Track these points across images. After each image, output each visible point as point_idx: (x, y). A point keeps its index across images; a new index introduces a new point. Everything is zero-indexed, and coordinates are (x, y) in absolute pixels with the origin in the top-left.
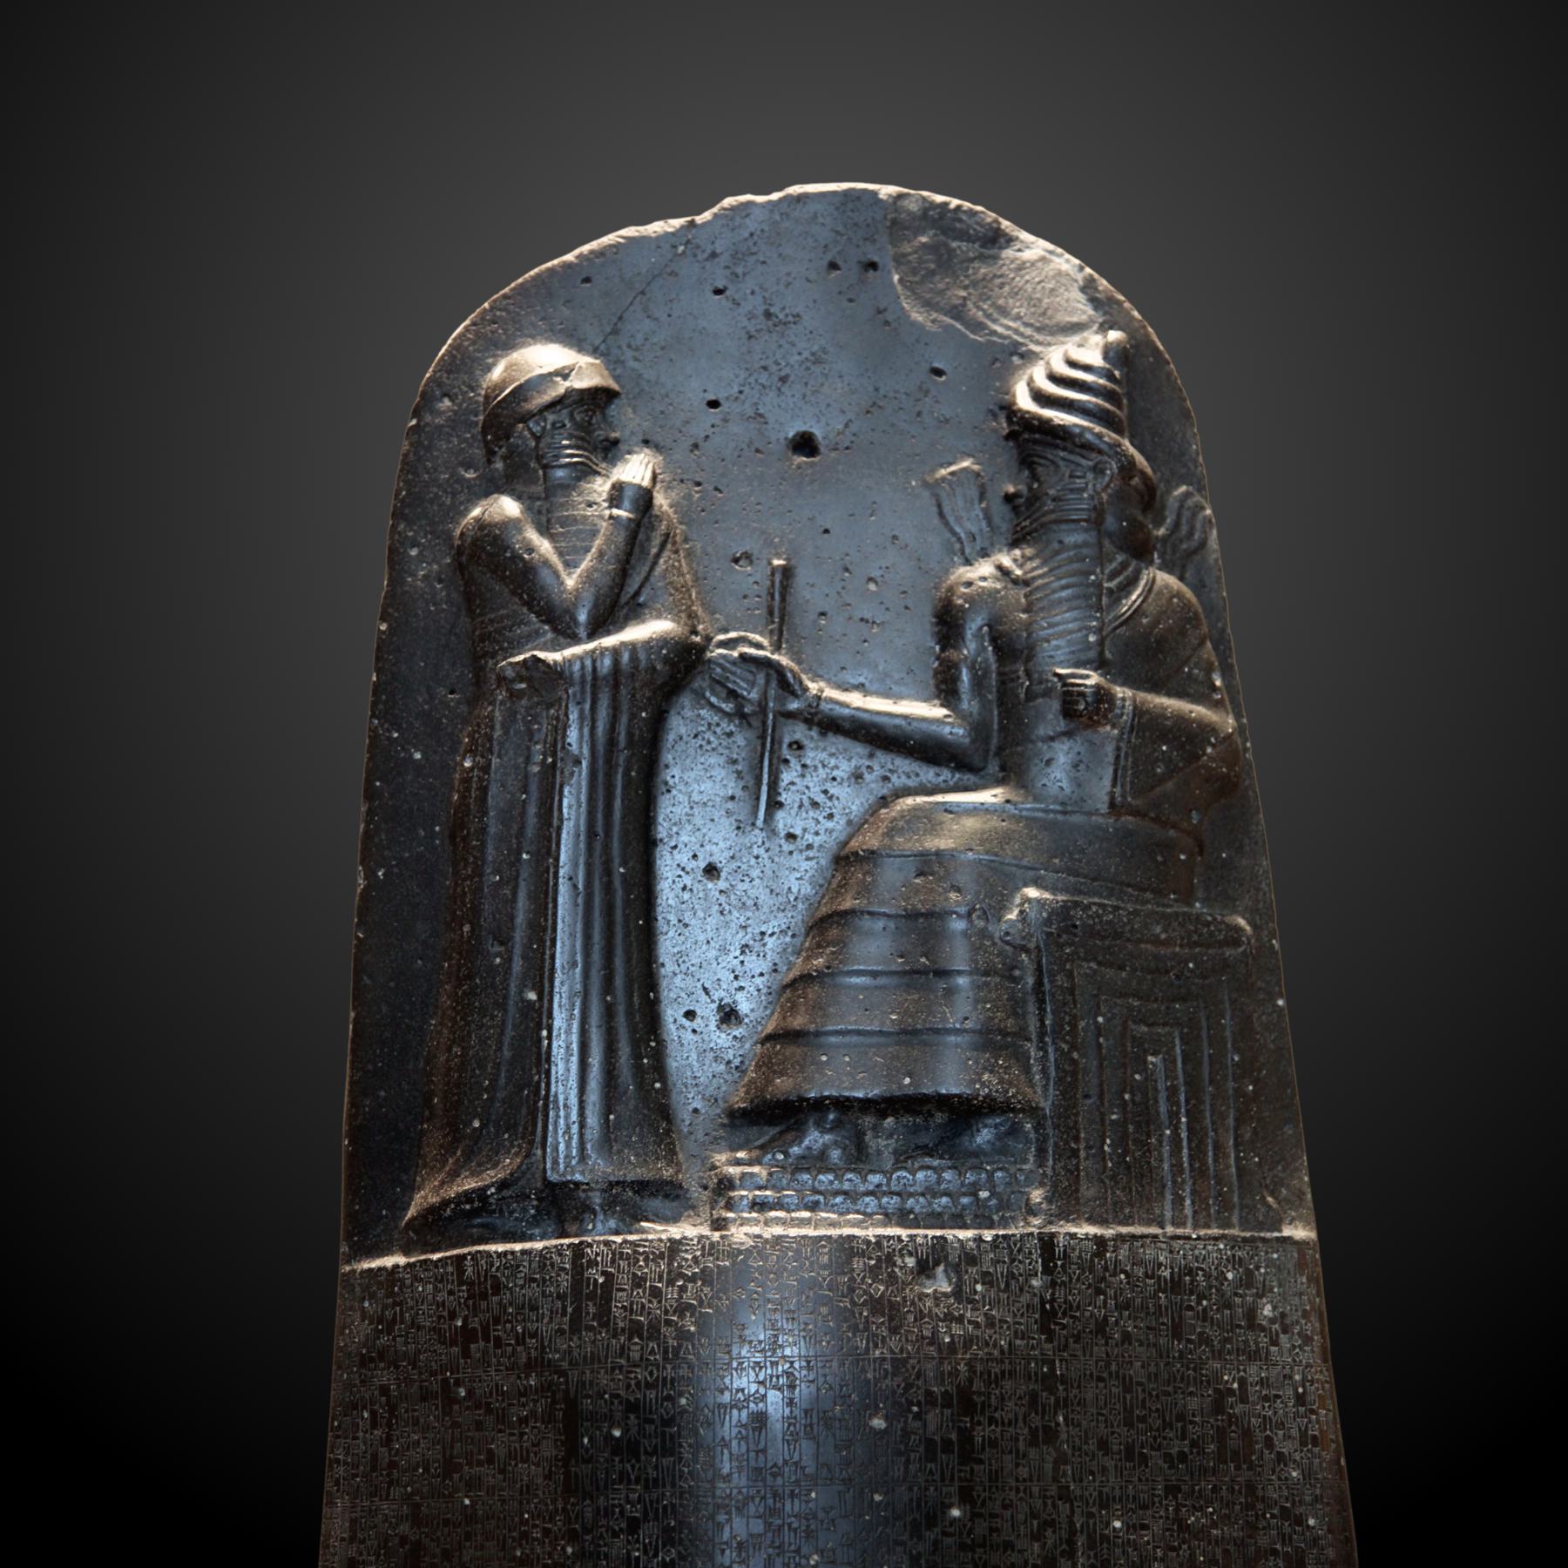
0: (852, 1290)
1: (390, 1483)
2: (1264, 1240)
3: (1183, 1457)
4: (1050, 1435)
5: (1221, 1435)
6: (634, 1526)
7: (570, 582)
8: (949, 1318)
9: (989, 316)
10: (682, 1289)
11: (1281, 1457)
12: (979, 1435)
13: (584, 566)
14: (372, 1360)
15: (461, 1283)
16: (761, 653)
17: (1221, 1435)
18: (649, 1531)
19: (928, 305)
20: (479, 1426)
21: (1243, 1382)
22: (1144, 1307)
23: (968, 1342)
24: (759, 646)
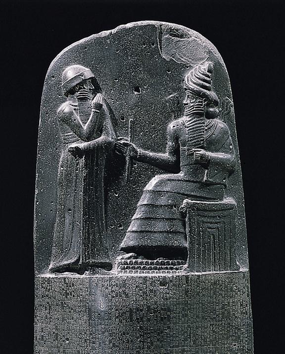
0: (146, 288)
1: (50, 322)
2: (235, 273)
3: (214, 318)
4: (186, 315)
5: (223, 313)
6: (103, 333)
7: (85, 127)
8: (166, 293)
9: (181, 57)
10: (112, 287)
11: (236, 317)
12: (172, 316)
13: (88, 123)
14: (45, 296)
15: (65, 283)
16: (127, 142)
17: (223, 313)
18: (106, 334)
19: (167, 53)
20: (70, 312)
21: (229, 303)
22: (207, 289)
23: (170, 298)
24: (127, 140)
